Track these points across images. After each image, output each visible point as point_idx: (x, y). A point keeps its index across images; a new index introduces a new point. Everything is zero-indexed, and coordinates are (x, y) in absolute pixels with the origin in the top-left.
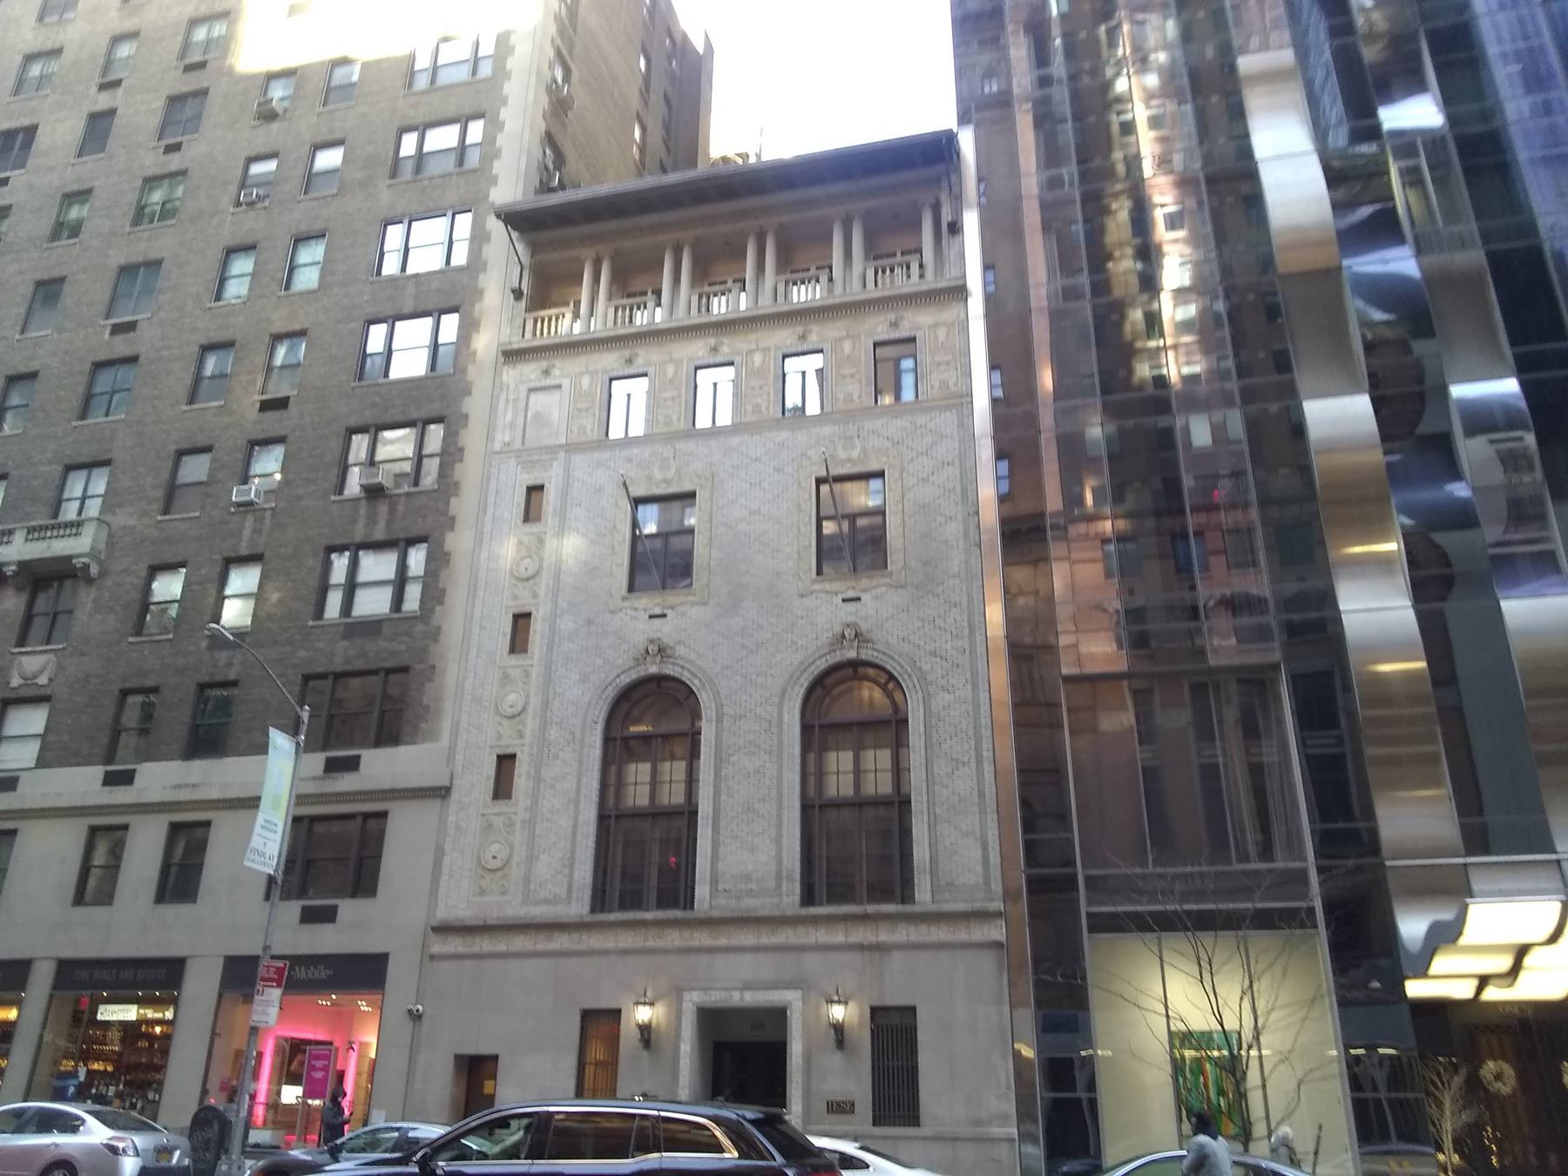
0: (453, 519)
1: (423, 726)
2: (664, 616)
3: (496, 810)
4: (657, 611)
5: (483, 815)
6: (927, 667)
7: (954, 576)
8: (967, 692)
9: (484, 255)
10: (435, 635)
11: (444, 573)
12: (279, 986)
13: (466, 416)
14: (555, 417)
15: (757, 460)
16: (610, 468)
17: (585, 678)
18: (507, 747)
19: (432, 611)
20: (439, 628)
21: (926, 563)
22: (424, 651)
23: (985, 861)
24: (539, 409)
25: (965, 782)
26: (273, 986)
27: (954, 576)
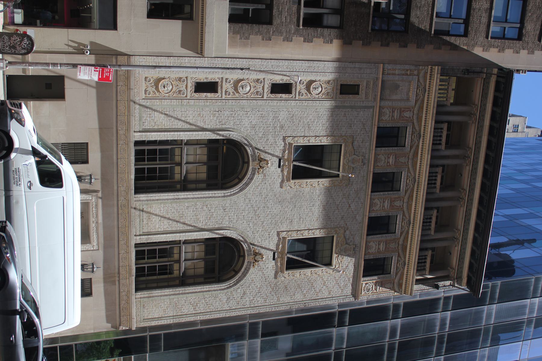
0: (350, 43)
1: (238, 36)
2: (279, 167)
3: (189, 85)
4: (282, 164)
5: (187, 78)
6: (239, 291)
7: (278, 300)
8: (226, 307)
9: (492, 49)
10: (288, 39)
11: (321, 40)
12: (99, 79)
13: (405, 46)
14: (394, 97)
15: (349, 206)
16: (361, 131)
17: (253, 127)
18: (222, 87)
19: (301, 36)
20: (291, 41)
21: (286, 287)
22: (281, 33)
23: (153, 319)
24: (401, 88)
25: (187, 309)
26: (99, 76)
27: (278, 300)
